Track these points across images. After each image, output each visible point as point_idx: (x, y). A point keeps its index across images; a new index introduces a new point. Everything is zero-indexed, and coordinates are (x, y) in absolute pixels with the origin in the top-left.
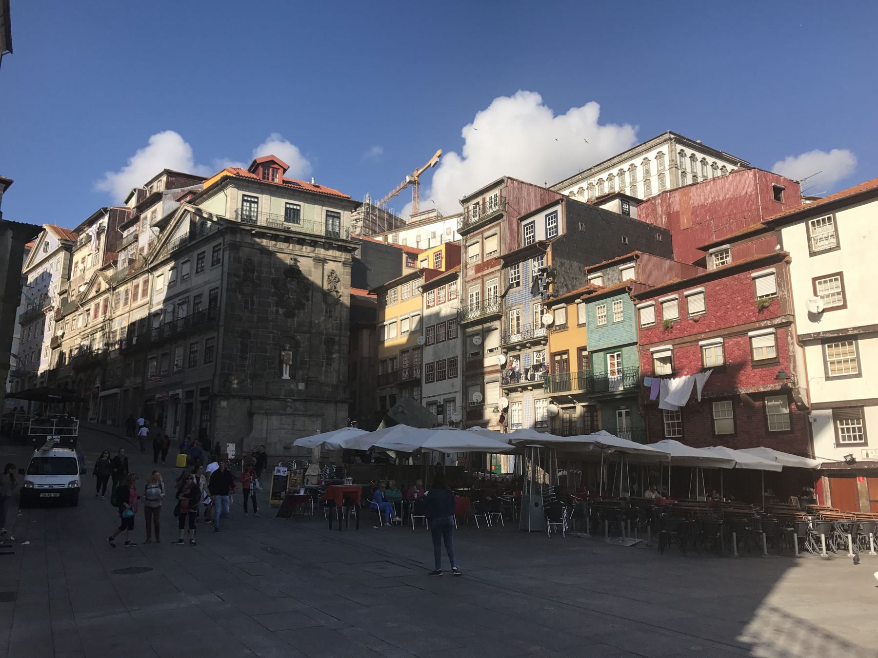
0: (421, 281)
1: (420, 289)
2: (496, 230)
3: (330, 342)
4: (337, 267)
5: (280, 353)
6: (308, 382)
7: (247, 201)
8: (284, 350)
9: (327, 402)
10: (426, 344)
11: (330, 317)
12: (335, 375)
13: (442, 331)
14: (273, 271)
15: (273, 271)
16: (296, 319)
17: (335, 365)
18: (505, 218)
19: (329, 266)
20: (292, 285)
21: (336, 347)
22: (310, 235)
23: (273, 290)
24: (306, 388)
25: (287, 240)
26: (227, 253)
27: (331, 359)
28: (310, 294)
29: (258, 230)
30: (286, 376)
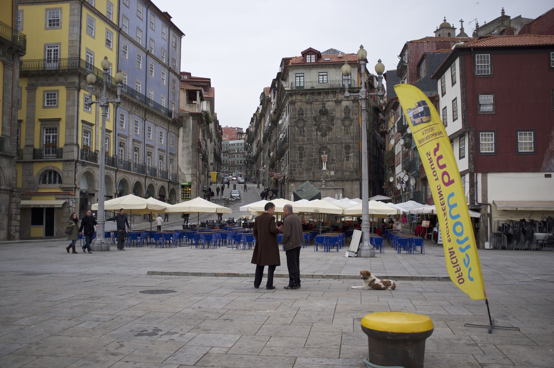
3: (348, 147)
7: (298, 76)
9: (347, 181)
10: (395, 144)
11: (347, 133)
14: (313, 112)
15: (313, 112)
16: (327, 137)
17: (351, 160)
19: (345, 103)
20: (324, 119)
21: (352, 150)
22: (331, 89)
25: (319, 94)
28: (335, 122)
30: (324, 168)
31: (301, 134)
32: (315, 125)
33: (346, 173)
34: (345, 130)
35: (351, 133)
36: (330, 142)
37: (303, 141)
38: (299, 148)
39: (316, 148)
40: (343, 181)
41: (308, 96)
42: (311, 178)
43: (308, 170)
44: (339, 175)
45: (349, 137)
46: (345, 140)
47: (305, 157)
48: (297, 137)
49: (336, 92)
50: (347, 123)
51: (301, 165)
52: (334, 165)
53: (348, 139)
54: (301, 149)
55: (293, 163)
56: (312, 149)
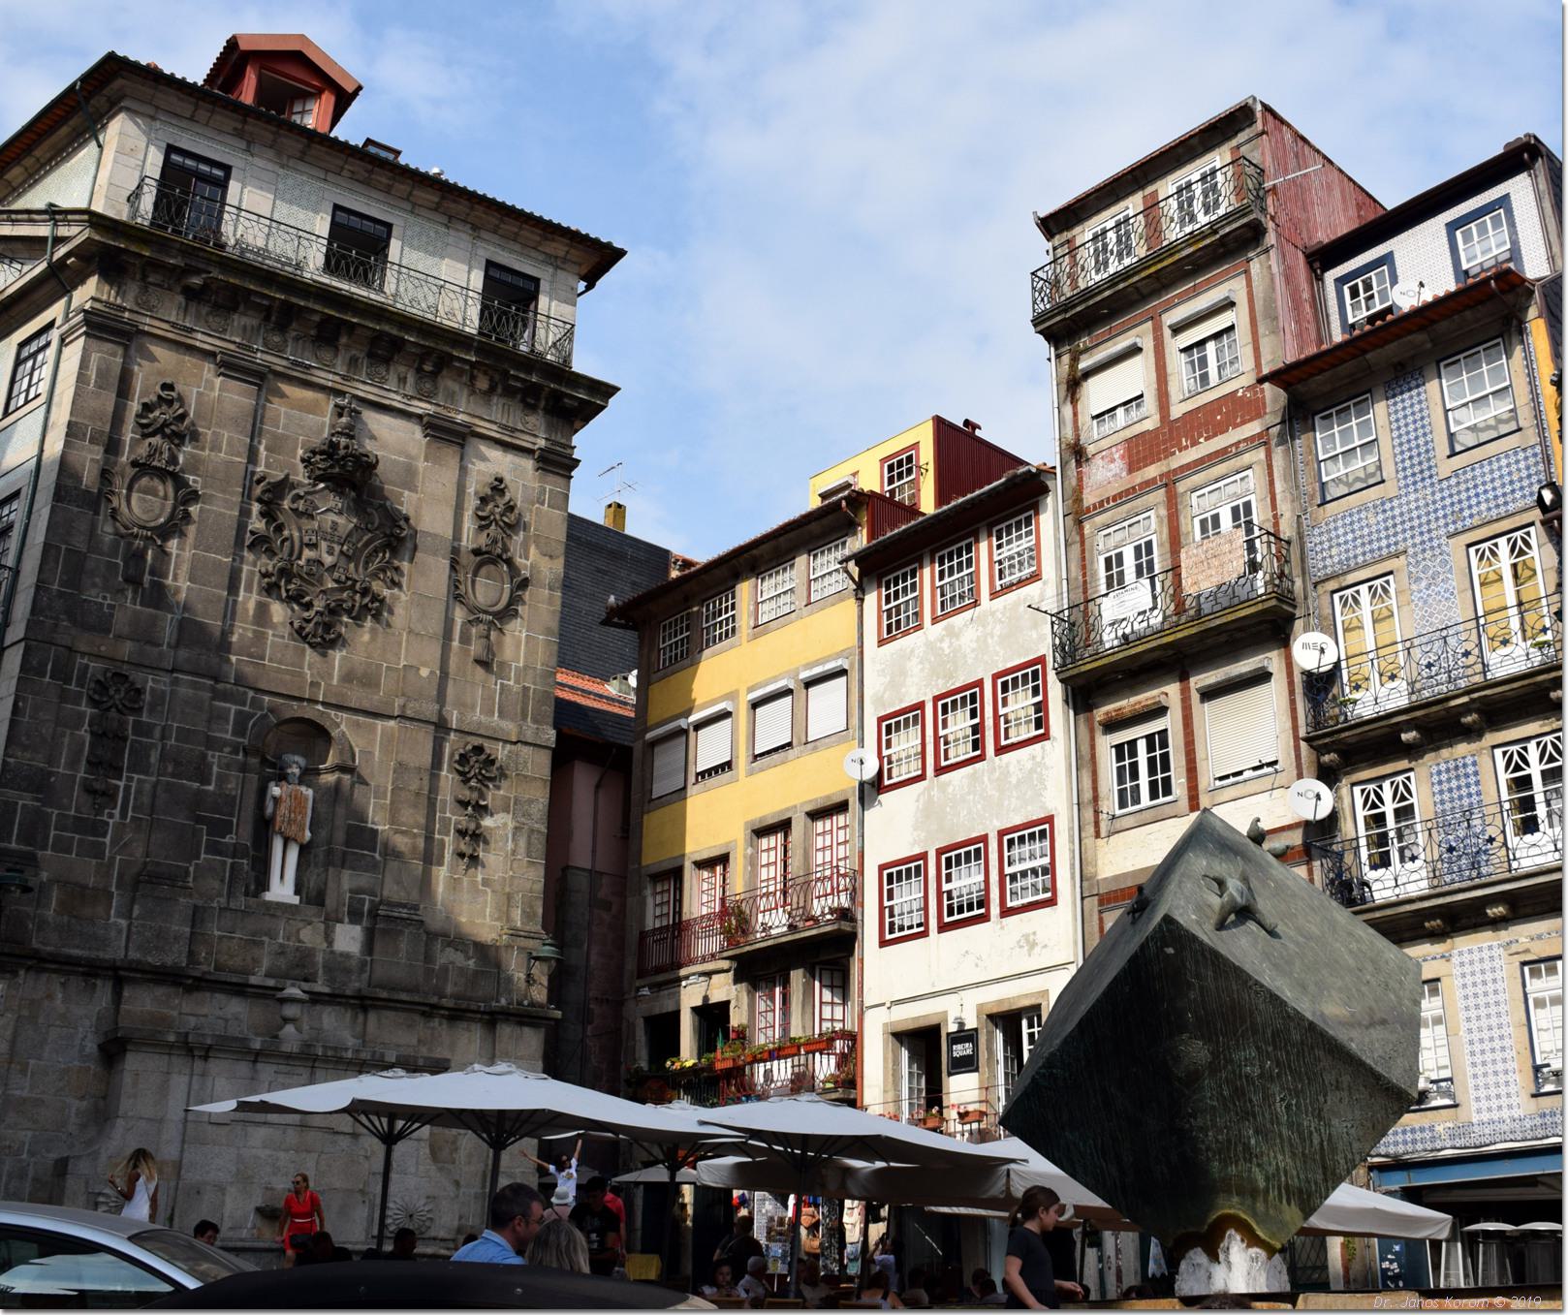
0: (859, 541)
1: (852, 567)
2: (1233, 287)
4: (519, 473)
5: (262, 791)
6: (382, 922)
8: (282, 777)
9: (457, 1015)
11: (478, 661)
12: (489, 900)
13: (960, 723)
16: (337, 656)
18: (1271, 238)
20: (332, 514)
23: (257, 524)
24: (369, 945)
26: (73, 353)
27: (477, 836)
29: (216, 273)
30: (282, 890)
31: (134, 581)
32: (260, 543)
33: (447, 956)
34: (465, 639)
35: (503, 671)
36: (356, 696)
37: (146, 636)
38: (102, 686)
39: (242, 720)
40: (429, 1011)
41: (239, 320)
42: (175, 956)
43: (150, 882)
44: (399, 961)
45: (488, 699)
46: (463, 706)
47: (140, 765)
48: (93, 595)
49: (443, 363)
50: (487, 590)
51: (99, 829)
52: (364, 880)
53: (477, 705)
54: (116, 693)
55: (25, 801)
56: (217, 717)
